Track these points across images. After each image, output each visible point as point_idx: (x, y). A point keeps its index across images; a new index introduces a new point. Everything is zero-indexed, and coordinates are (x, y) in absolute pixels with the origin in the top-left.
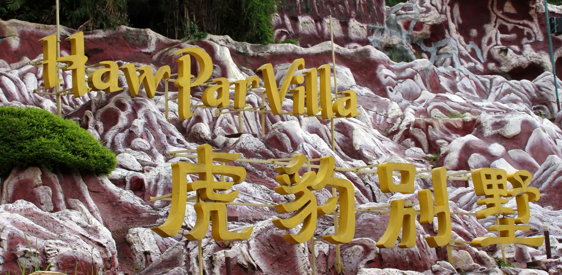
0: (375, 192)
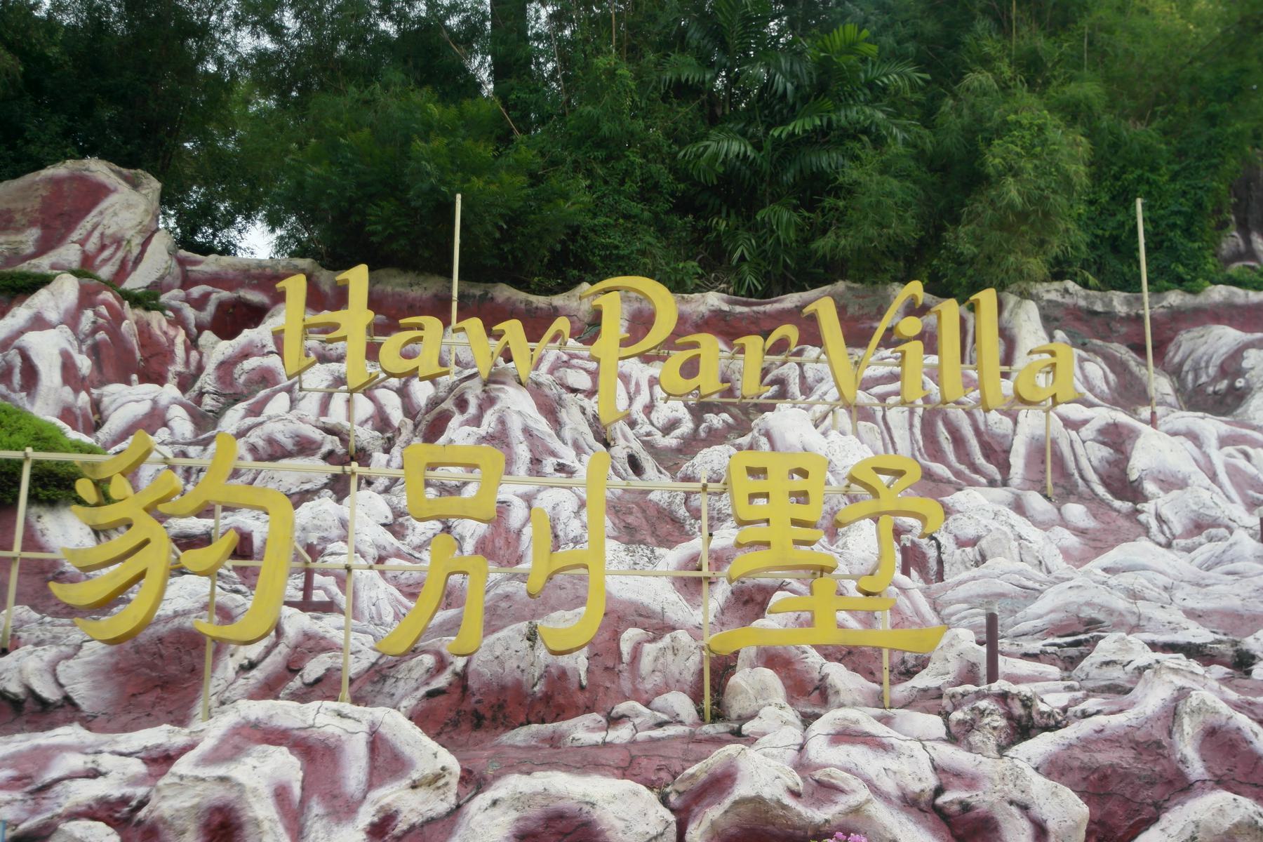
0: (944, 557)
